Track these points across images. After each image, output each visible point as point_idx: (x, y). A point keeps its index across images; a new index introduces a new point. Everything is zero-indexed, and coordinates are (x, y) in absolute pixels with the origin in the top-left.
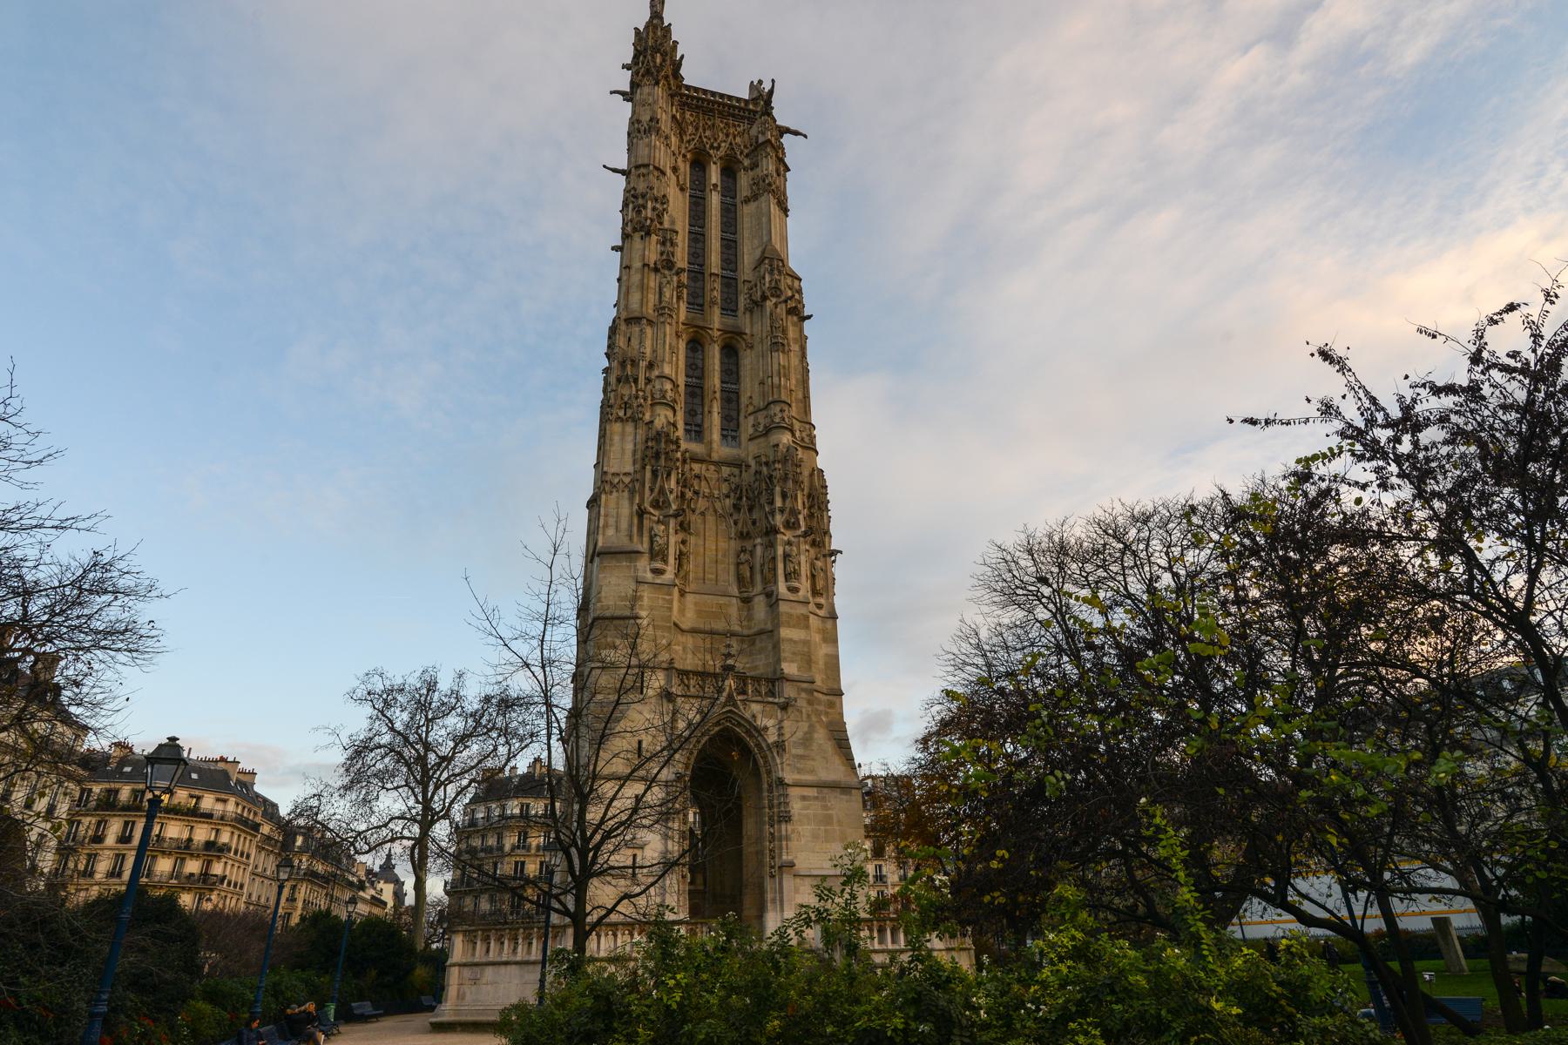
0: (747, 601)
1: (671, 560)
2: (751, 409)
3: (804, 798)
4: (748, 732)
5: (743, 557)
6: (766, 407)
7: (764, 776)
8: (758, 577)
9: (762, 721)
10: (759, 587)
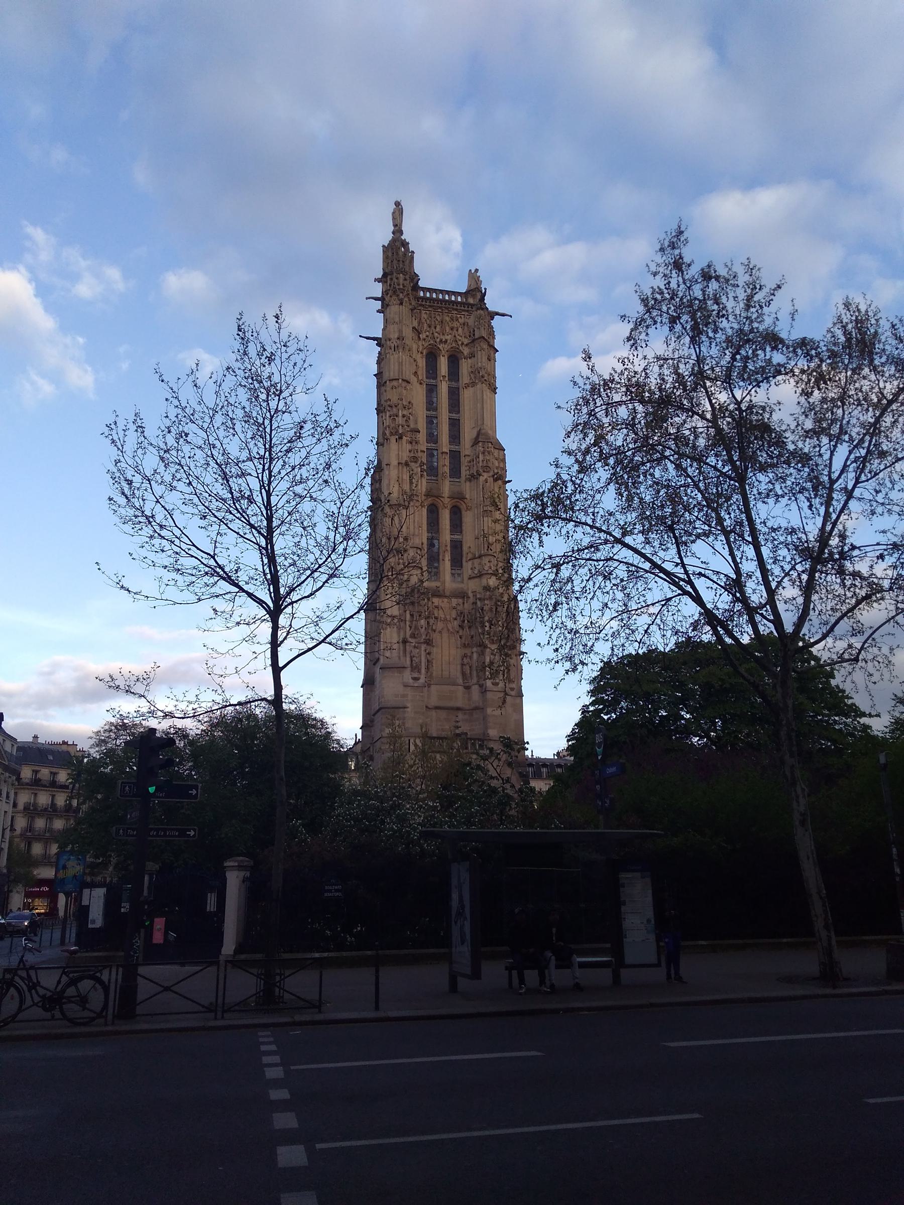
0: (468, 688)
1: (423, 671)
2: (470, 556)
5: (465, 661)
6: (480, 557)
10: (475, 680)
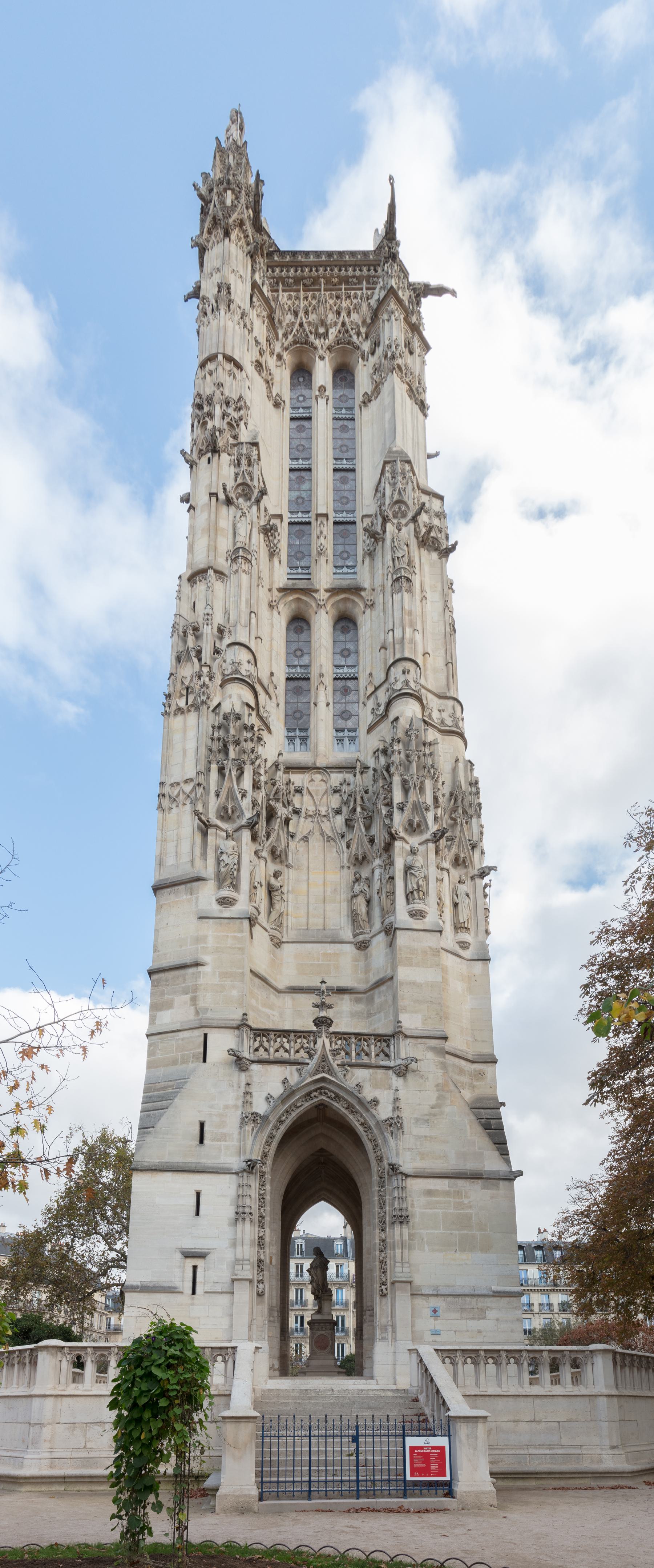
3: (429, 1193)
4: (350, 1107)
8: (376, 912)
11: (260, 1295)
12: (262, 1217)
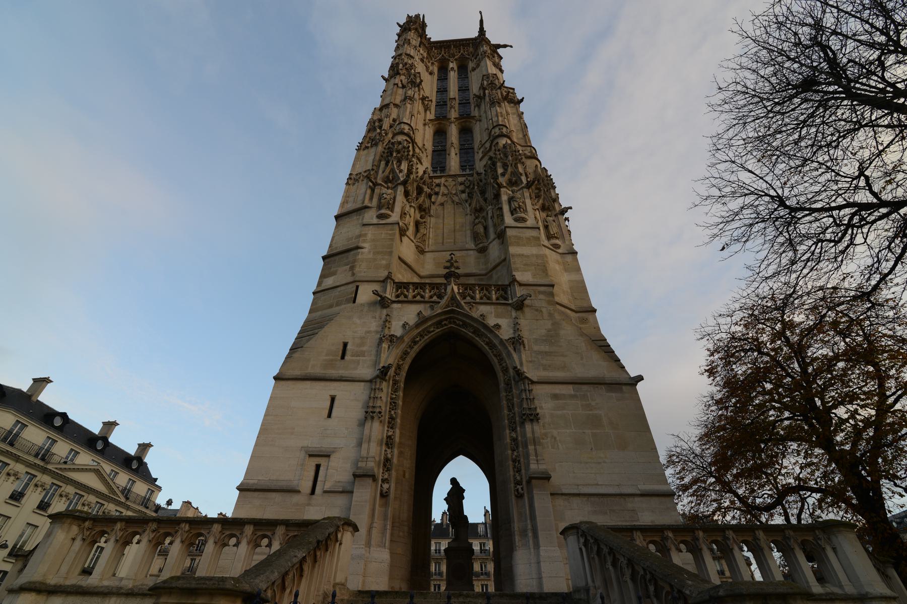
7: (500, 375)
9: (491, 321)
11: (384, 495)
12: (392, 418)
